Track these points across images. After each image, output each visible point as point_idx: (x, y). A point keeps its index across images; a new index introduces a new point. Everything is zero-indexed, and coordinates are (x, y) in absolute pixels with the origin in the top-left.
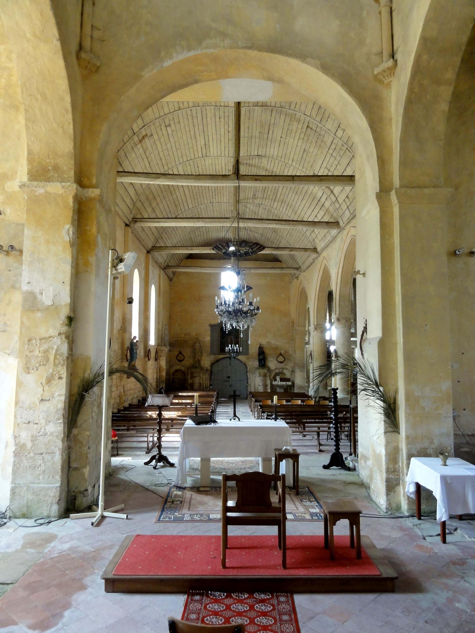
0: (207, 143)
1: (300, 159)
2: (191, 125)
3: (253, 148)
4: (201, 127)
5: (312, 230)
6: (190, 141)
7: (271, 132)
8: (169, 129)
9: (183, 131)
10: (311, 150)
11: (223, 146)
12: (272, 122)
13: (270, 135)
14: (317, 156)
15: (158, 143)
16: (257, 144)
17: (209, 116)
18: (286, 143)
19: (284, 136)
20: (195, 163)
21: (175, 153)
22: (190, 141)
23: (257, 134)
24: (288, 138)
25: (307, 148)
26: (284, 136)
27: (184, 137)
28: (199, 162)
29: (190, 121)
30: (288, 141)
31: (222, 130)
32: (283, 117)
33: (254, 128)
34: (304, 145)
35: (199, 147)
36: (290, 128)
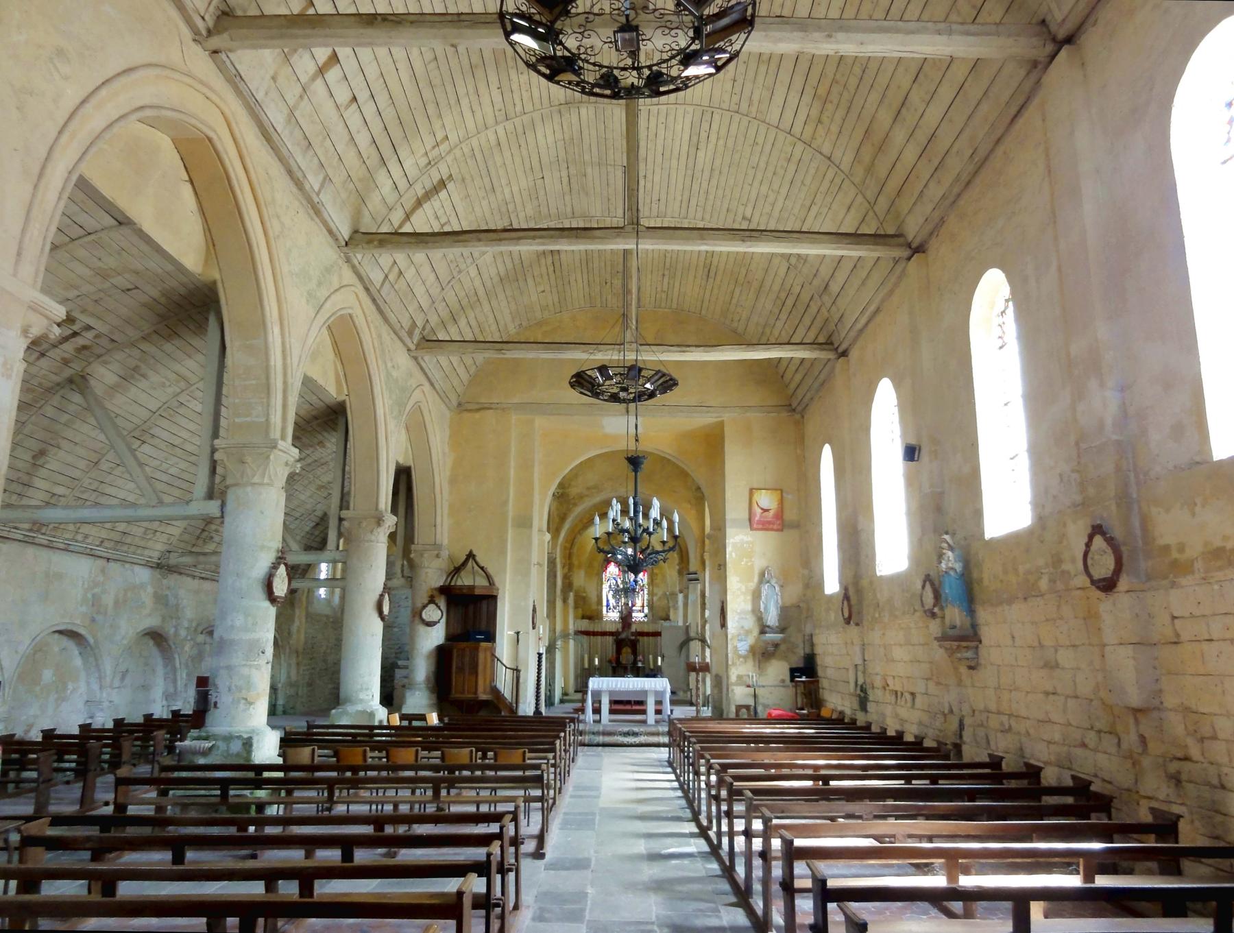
0: (693, 150)
1: (490, 163)
2: (711, 197)
3: (593, 132)
4: (696, 187)
5: (322, 54)
6: (725, 170)
7: (565, 180)
8: (748, 215)
9: (728, 192)
10: (485, 203)
11: (660, 141)
12: (567, 198)
13: (564, 174)
14: (471, 210)
15: (776, 213)
16: (586, 147)
17: (678, 204)
18: (528, 171)
19: (539, 182)
20: (735, 98)
21: (762, 165)
22: (725, 170)
23: (589, 170)
24: (531, 184)
25: (492, 198)
26: (539, 182)
27: (731, 182)
28: (726, 97)
29: (710, 203)
30: (529, 180)
31: (657, 179)
32: (553, 211)
33: (597, 182)
34: (500, 197)
35: (711, 146)
36: (535, 203)
